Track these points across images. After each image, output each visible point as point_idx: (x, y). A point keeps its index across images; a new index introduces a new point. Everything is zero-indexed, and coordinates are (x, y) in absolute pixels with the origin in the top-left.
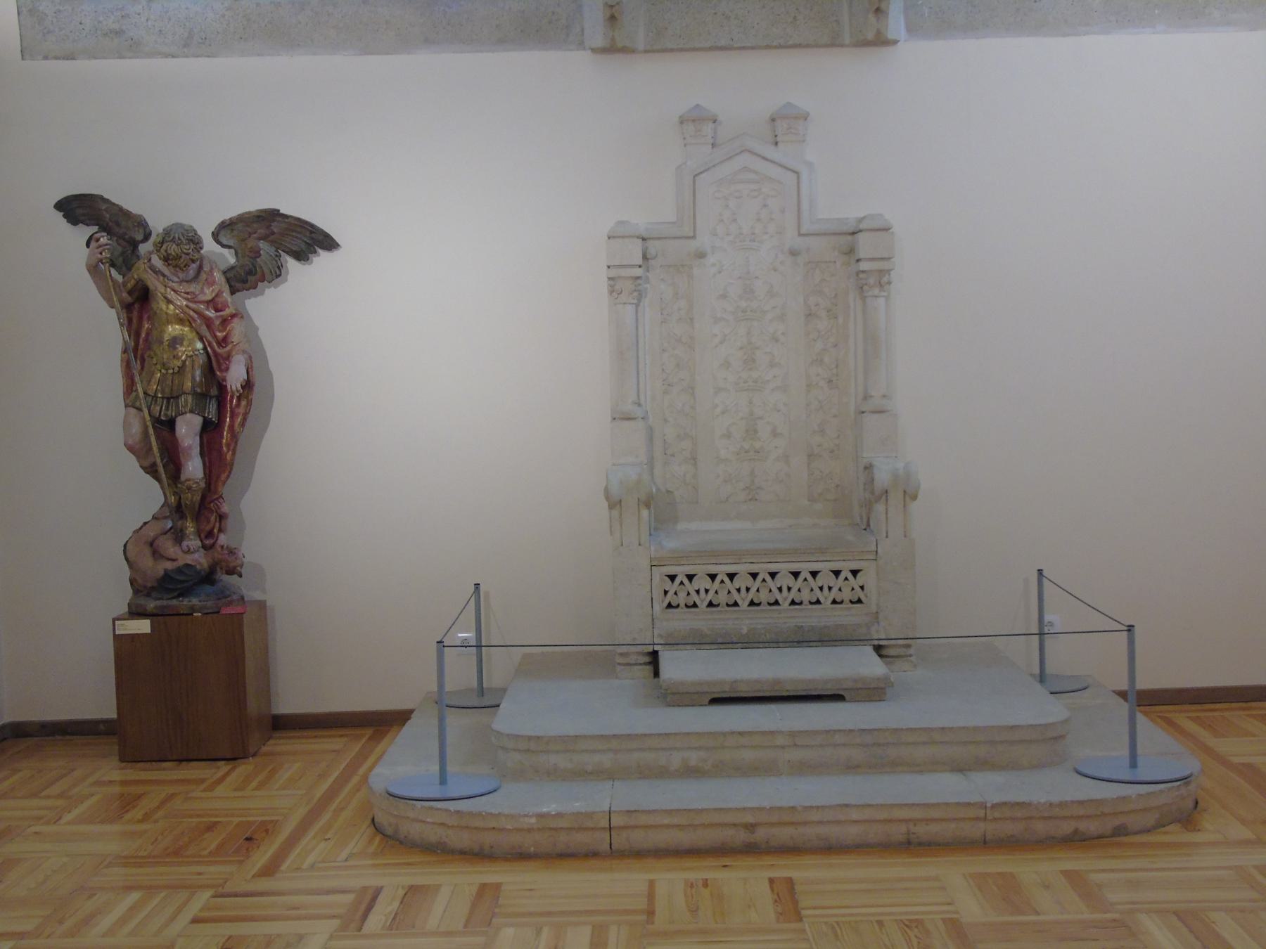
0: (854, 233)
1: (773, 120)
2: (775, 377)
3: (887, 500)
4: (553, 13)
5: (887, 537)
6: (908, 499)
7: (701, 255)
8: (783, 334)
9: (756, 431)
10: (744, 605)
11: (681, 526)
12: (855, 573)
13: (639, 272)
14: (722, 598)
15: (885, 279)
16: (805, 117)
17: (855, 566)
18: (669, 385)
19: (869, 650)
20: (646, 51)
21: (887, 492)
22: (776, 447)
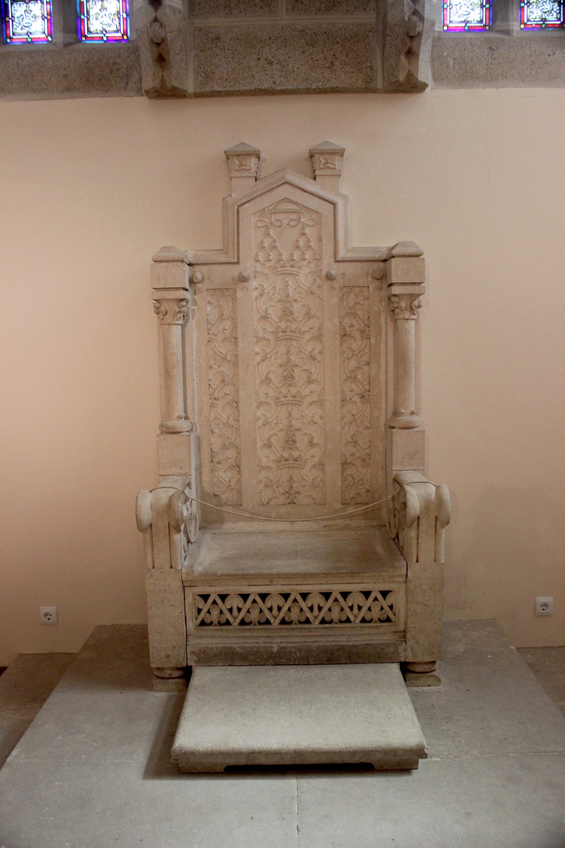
0: (385, 261)
1: (312, 156)
2: (312, 392)
3: (418, 525)
4: (114, 63)
5: (417, 561)
6: (439, 524)
7: (243, 279)
8: (320, 352)
9: (294, 441)
10: (276, 623)
11: (228, 526)
12: (385, 594)
13: (181, 294)
14: (254, 616)
15: (416, 303)
16: (340, 153)
17: (384, 587)
18: (215, 399)
19: (395, 668)
20: (198, 95)
21: (418, 518)
22: (313, 456)
